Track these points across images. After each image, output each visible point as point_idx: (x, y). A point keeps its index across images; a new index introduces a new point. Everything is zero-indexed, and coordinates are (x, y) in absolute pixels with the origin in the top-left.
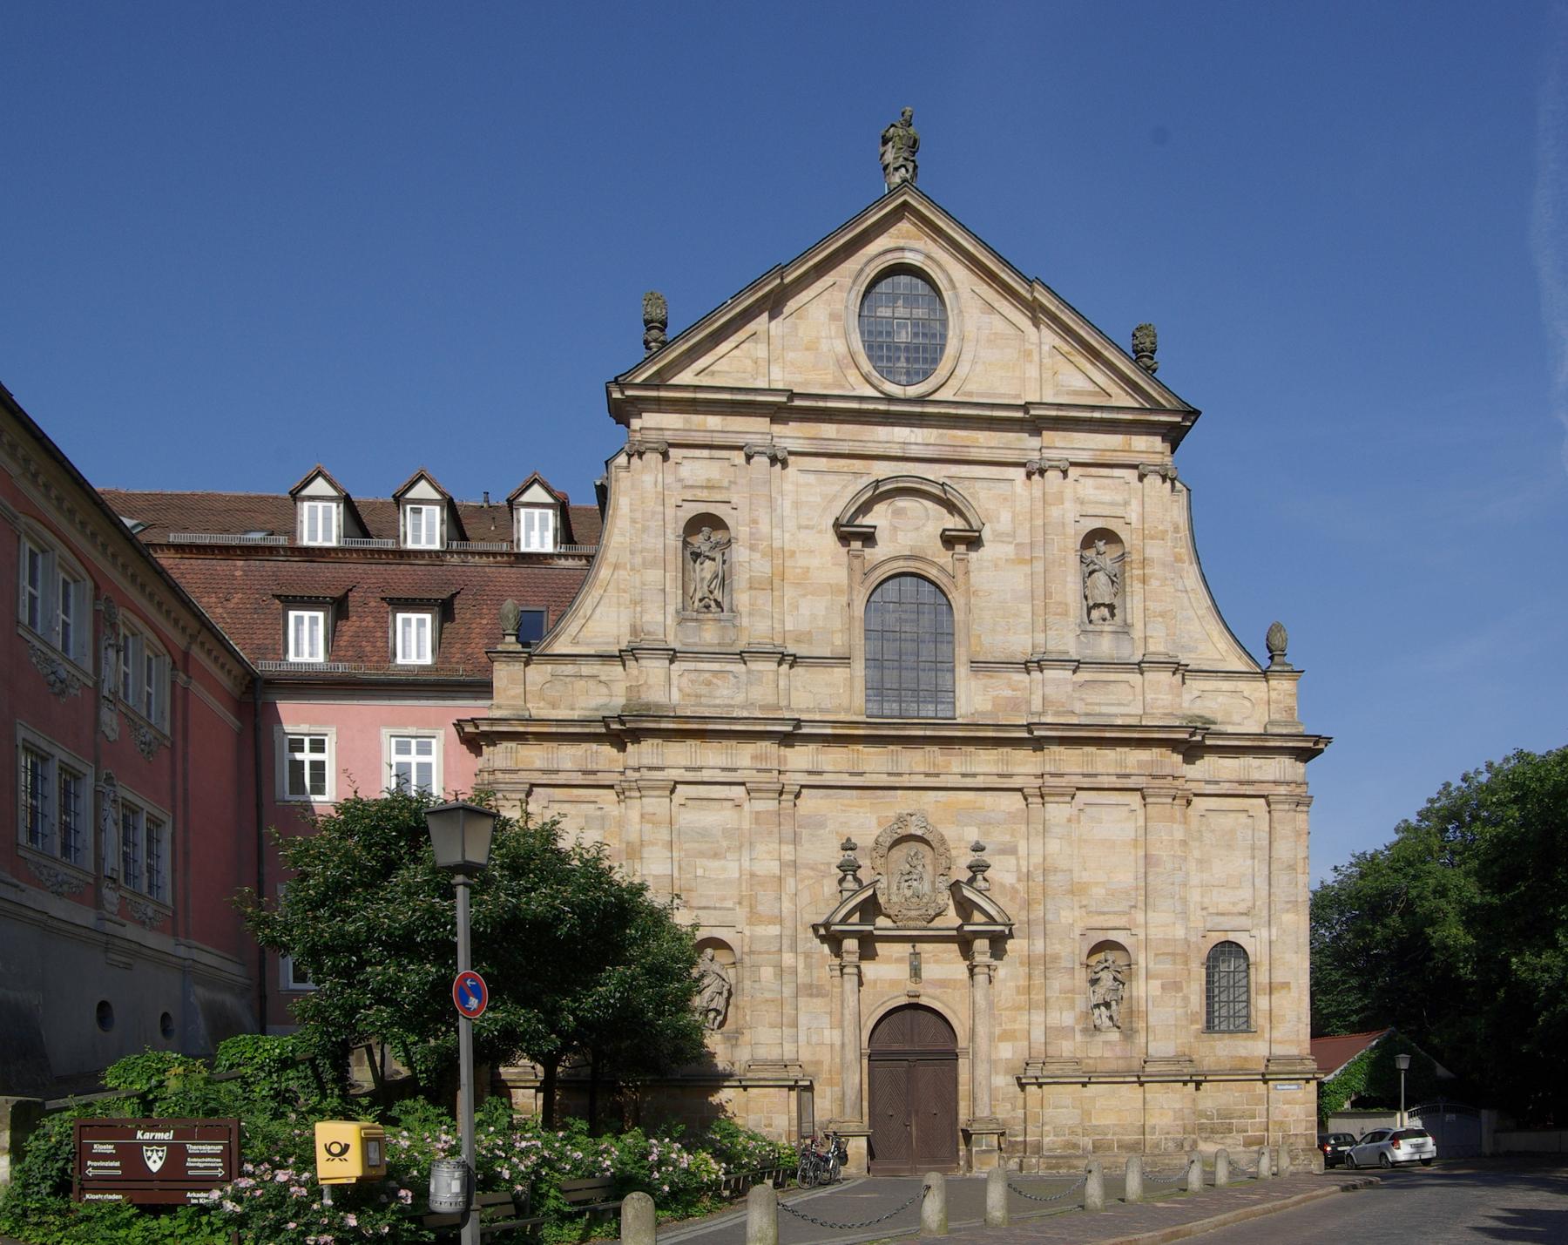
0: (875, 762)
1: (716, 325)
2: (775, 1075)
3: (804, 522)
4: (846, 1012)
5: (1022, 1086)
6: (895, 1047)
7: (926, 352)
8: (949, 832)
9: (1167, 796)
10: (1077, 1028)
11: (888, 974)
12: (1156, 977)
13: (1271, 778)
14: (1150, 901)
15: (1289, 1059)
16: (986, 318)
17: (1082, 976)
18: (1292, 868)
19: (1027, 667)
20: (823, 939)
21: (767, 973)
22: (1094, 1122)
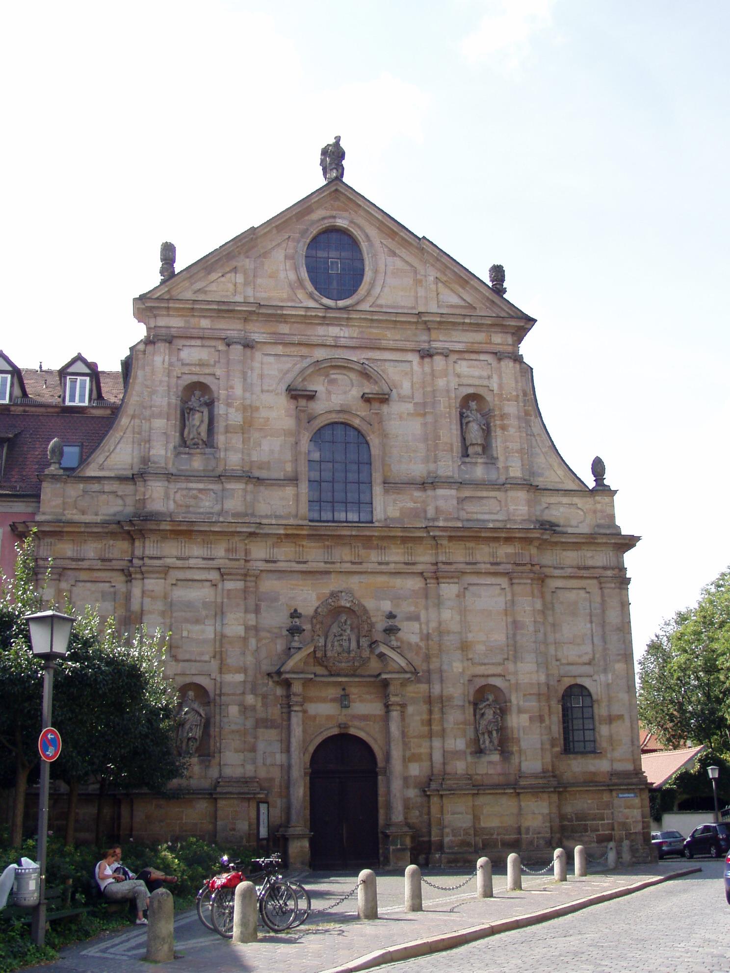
0: (315, 555)
9: (527, 578)
10: (469, 751)
12: (525, 712)
16: (390, 260)
20: (277, 683)
21: (234, 710)
22: (483, 825)
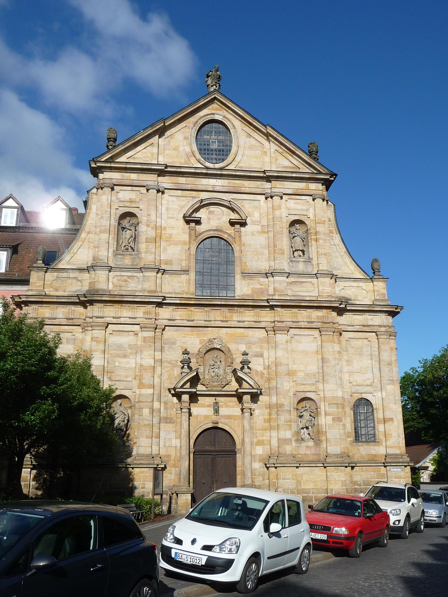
0: (199, 316)
1: (136, 140)
2: (148, 462)
3: (170, 216)
4: (183, 431)
5: (268, 468)
6: (207, 448)
7: (224, 152)
8: (232, 347)
9: (330, 331)
10: (293, 439)
11: (203, 411)
13: (378, 324)
14: (326, 378)
15: (395, 456)
17: (294, 414)
18: (390, 364)
19: (266, 275)
20: (173, 395)
21: (146, 411)
